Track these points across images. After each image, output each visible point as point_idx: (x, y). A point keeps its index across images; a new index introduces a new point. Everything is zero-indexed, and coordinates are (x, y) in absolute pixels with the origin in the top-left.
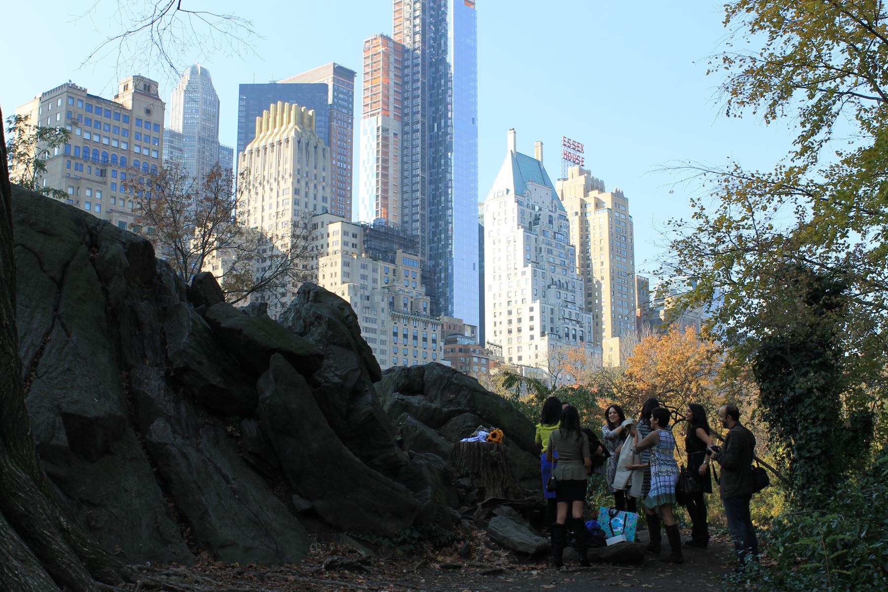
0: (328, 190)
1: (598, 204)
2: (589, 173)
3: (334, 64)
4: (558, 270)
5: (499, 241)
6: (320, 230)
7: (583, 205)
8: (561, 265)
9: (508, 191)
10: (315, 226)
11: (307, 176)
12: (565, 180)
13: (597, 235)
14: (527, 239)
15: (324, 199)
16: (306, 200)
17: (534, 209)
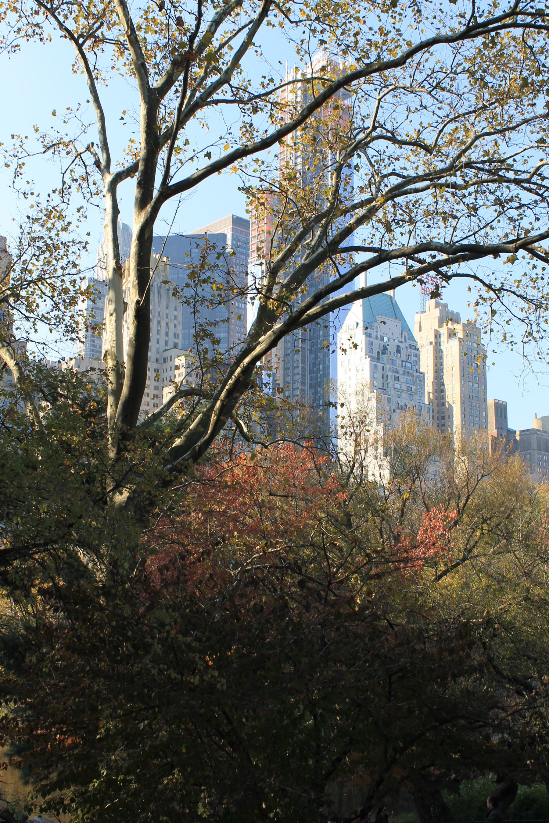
0: (180, 328)
1: (452, 334)
2: (446, 306)
3: (233, 216)
4: (405, 395)
5: (350, 370)
6: (169, 364)
7: (438, 336)
8: (407, 390)
9: (357, 324)
10: (165, 360)
11: (159, 315)
12: (423, 312)
13: (449, 363)
14: (373, 368)
15: (176, 336)
16: (158, 336)
17: (382, 339)
